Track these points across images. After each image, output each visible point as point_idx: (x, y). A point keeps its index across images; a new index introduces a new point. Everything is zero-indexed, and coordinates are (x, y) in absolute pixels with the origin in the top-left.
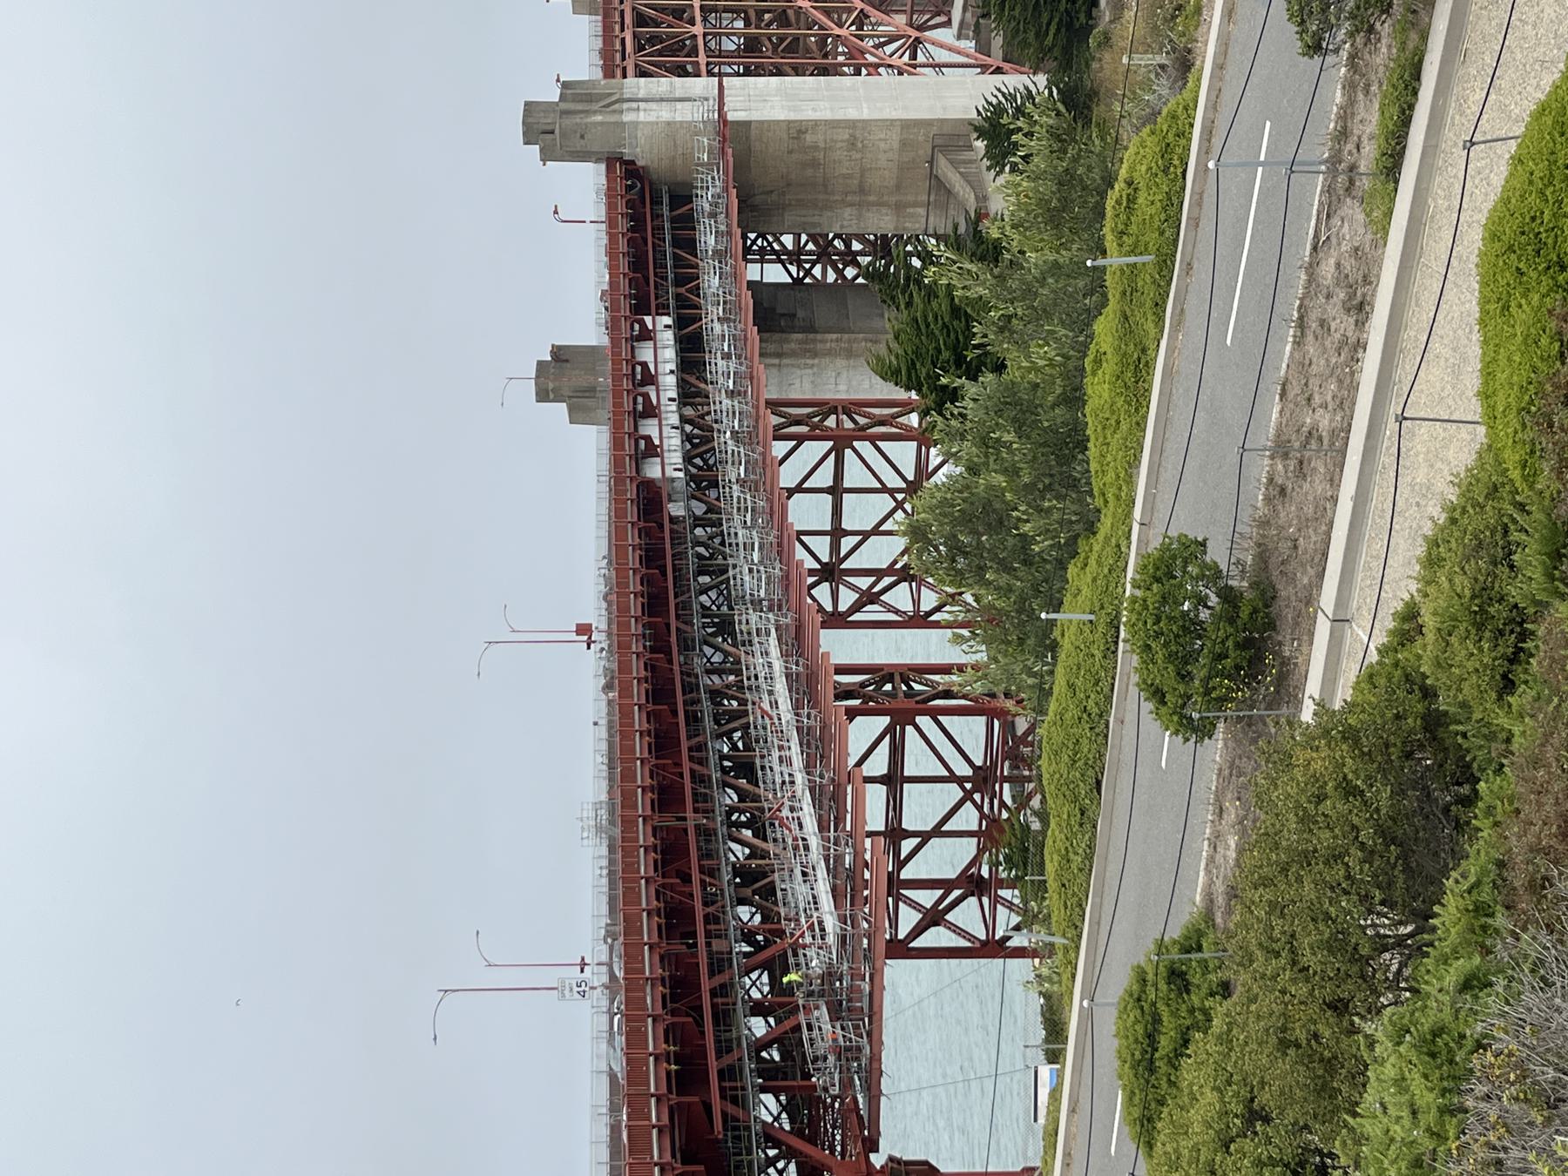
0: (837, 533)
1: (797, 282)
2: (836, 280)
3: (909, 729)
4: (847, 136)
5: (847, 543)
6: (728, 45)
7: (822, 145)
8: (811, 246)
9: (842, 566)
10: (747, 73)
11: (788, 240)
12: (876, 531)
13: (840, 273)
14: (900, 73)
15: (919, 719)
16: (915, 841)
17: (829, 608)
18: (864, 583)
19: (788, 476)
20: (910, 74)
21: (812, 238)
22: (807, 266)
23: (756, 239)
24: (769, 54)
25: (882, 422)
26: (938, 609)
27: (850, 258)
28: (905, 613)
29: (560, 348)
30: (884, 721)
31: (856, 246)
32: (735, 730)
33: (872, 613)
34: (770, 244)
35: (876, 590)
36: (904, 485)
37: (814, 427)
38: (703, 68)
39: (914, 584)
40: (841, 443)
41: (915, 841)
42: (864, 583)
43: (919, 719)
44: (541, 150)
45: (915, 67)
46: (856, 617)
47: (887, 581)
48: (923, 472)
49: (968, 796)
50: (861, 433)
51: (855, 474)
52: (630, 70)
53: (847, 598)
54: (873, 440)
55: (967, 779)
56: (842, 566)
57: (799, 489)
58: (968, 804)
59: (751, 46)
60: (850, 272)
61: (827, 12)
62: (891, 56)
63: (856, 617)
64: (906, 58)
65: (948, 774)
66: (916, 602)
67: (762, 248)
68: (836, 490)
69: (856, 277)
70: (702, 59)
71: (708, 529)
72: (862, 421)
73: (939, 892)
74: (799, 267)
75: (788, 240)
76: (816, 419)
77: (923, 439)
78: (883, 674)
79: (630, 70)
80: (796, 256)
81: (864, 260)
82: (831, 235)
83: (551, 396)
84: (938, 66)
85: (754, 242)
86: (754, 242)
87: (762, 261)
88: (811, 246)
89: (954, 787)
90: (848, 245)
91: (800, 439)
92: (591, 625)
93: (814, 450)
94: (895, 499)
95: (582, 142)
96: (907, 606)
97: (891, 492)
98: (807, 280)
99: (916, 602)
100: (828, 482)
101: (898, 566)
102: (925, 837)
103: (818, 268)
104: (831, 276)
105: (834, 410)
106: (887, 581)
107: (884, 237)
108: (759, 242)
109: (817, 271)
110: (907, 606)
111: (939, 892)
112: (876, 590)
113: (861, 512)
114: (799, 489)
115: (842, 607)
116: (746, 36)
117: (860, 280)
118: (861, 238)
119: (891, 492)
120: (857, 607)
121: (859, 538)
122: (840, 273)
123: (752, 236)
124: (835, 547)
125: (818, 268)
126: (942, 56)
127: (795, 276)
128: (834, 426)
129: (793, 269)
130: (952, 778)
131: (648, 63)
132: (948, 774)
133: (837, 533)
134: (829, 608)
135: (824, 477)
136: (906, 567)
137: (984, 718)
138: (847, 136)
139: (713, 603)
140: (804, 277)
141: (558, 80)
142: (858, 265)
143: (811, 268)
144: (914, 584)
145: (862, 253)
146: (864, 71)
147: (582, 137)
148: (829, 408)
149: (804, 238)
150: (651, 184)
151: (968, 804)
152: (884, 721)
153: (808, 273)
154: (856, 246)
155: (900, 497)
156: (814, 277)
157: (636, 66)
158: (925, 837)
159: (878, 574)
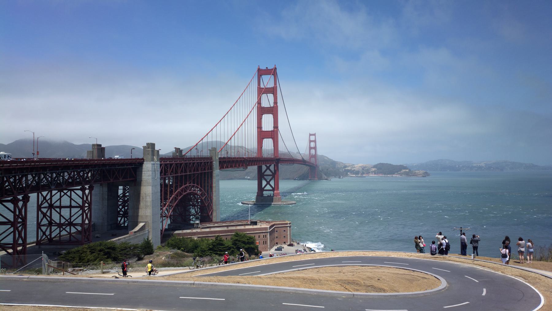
0: (60, 207)
1: (119, 196)
2: (119, 204)
3: (10, 226)
4: (148, 205)
5: (58, 210)
6: (167, 181)
7: (147, 200)
8: (126, 199)
9: (53, 209)
10: (161, 185)
11: (127, 194)
12: (61, 216)
13: (120, 205)
14: (161, 214)
15: (81, 210)
16: (59, 211)
17: (42, 206)
18: (48, 214)
19: (74, 196)
20: (161, 216)
21: (128, 199)
22: (122, 198)
23: (128, 188)
24: (165, 189)
25: (87, 215)
26: (42, 230)
27: (123, 207)
28: (41, 223)
29: (105, 149)
30: (12, 220)
31: (126, 208)
32: (10, 186)
33: (41, 216)
34: (127, 191)
35: (46, 216)
36: (72, 221)
37: (85, 201)
38: (162, 177)
39: (48, 225)
40: (82, 207)
41: (59, 211)
42: (48, 214)
43: (81, 210)
44: (145, 146)
45: (162, 217)
46: (40, 213)
47: (49, 219)
48: (74, 225)
49: (67, 220)
50: (84, 211)
51: (74, 211)
52: (161, 163)
53: (44, 210)
54: (82, 214)
55: (70, 220)
56: (53, 209)
57: (71, 199)
58: (65, 221)
59: (166, 185)
60: (121, 207)
61: (172, 199)
62: (164, 212)
63: (40, 213)
64: (164, 215)
65: (13, 233)
66: (43, 225)
67: (126, 189)
68: (71, 207)
69: (119, 208)
70: (164, 176)
71: (62, 180)
72: (87, 211)
73: (49, 216)
74: (122, 197)
75: (127, 194)
76: (87, 202)
77: (82, 225)
78: (24, 219)
79: (161, 163)
80: (124, 196)
81: (123, 210)
82: (128, 203)
83: (94, 147)
84: (162, 222)
85: (127, 187)
86: (127, 187)
87: (123, 189)
88: (126, 199)
89: (69, 217)
90: (126, 206)
91: (83, 198)
92: (39, 155)
93: (80, 201)
94: (68, 219)
95: (147, 154)
96: (42, 223)
97: (70, 219)
98: (119, 198)
99: (43, 225)
100: (72, 205)
101: (53, 221)
102: (60, 213)
103: (122, 200)
104: (120, 203)
105: (89, 205)
106: (49, 219)
107: (128, 213)
108: (127, 188)
109: (121, 200)
110: (42, 223)
111: (49, 216)
112: (46, 216)
113: (65, 213)
114: (71, 199)
115: (42, 210)
116: (168, 185)
117: (119, 210)
118: (128, 209)
119: (70, 219)
120: (42, 212)
121: (59, 212)
122: (120, 205)
123: (128, 187)
124: (57, 207)
125: (122, 200)
126: (164, 222)
127: (120, 196)
128: (86, 205)
129: (121, 195)
130: (71, 217)
131: (163, 167)
132: (13, 233)
133: (60, 207)
134: (42, 206)
135: (73, 204)
136: (52, 223)
137: (12, 242)
138: (148, 205)
139: (44, 181)
140: (120, 198)
141: (160, 150)
142: (122, 208)
143: (122, 199)
144: (48, 225)
145: (125, 209)
146: (161, 207)
147: (148, 154)
148: (90, 204)
149: (128, 197)
150: (139, 167)
151: (65, 221)
152: (12, 220)
153: (121, 199)
154: (126, 208)
155: (69, 220)
156: (120, 200)
157: (162, 164)
158: (60, 213)
159: (51, 217)
